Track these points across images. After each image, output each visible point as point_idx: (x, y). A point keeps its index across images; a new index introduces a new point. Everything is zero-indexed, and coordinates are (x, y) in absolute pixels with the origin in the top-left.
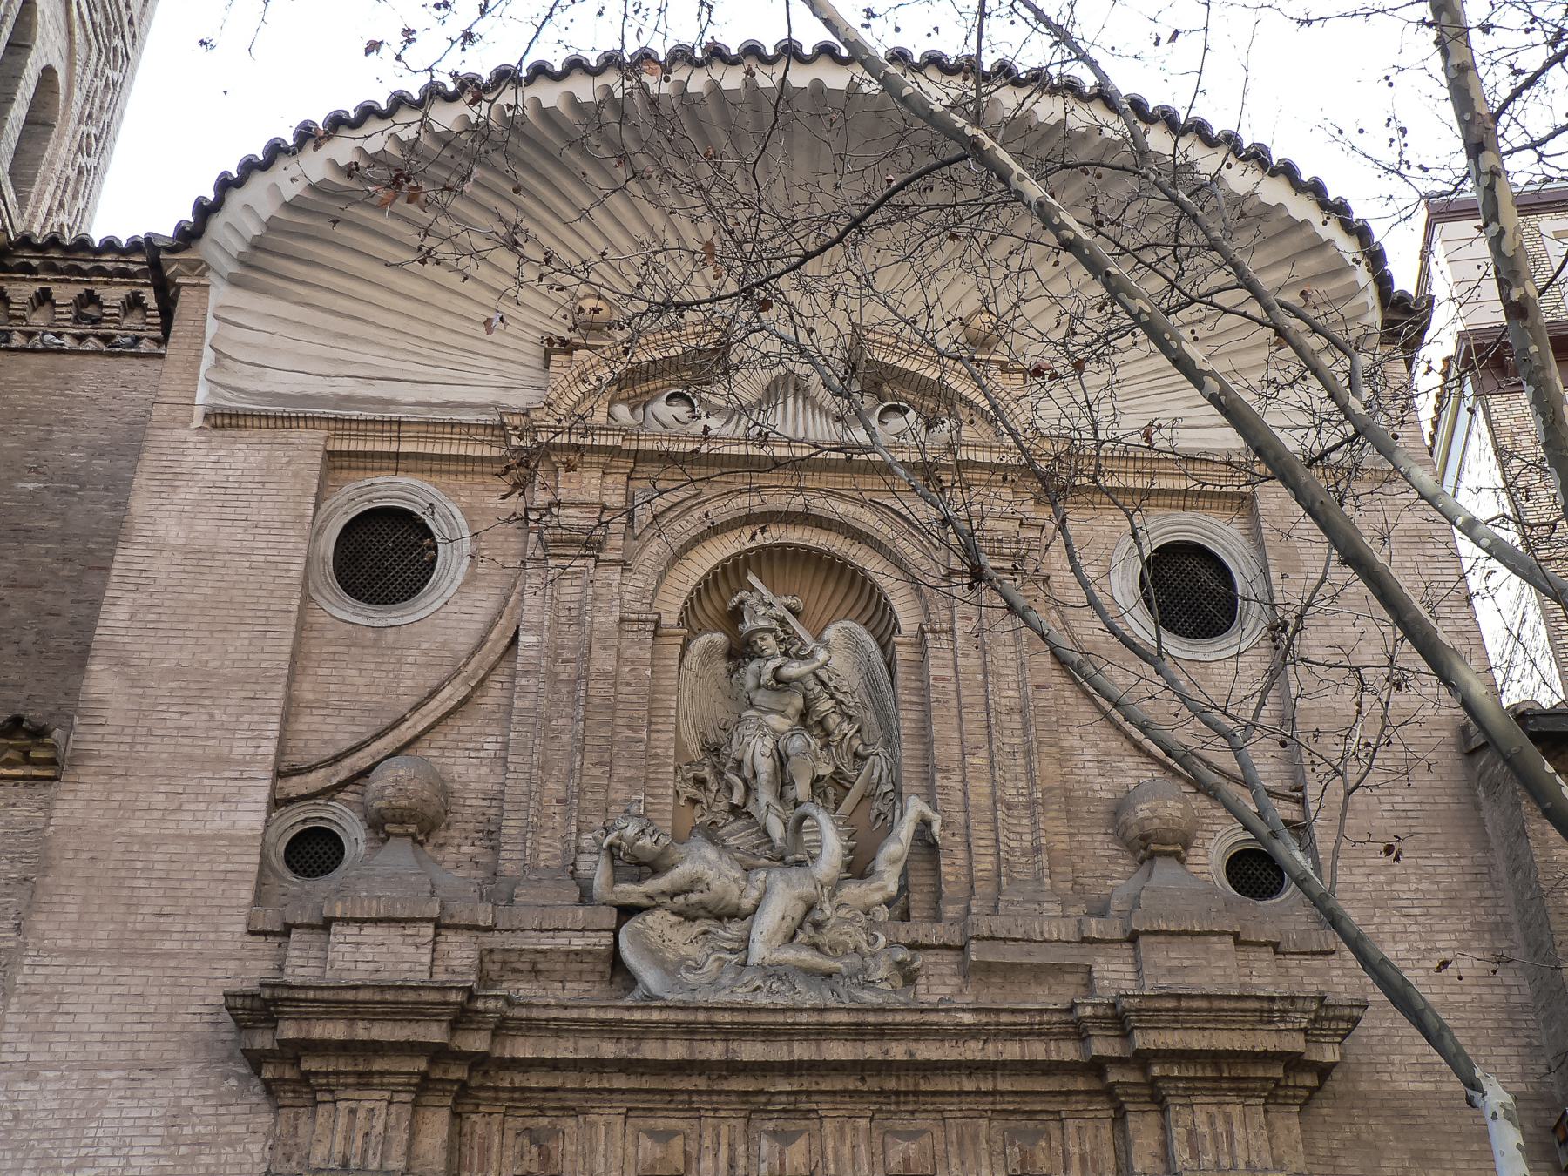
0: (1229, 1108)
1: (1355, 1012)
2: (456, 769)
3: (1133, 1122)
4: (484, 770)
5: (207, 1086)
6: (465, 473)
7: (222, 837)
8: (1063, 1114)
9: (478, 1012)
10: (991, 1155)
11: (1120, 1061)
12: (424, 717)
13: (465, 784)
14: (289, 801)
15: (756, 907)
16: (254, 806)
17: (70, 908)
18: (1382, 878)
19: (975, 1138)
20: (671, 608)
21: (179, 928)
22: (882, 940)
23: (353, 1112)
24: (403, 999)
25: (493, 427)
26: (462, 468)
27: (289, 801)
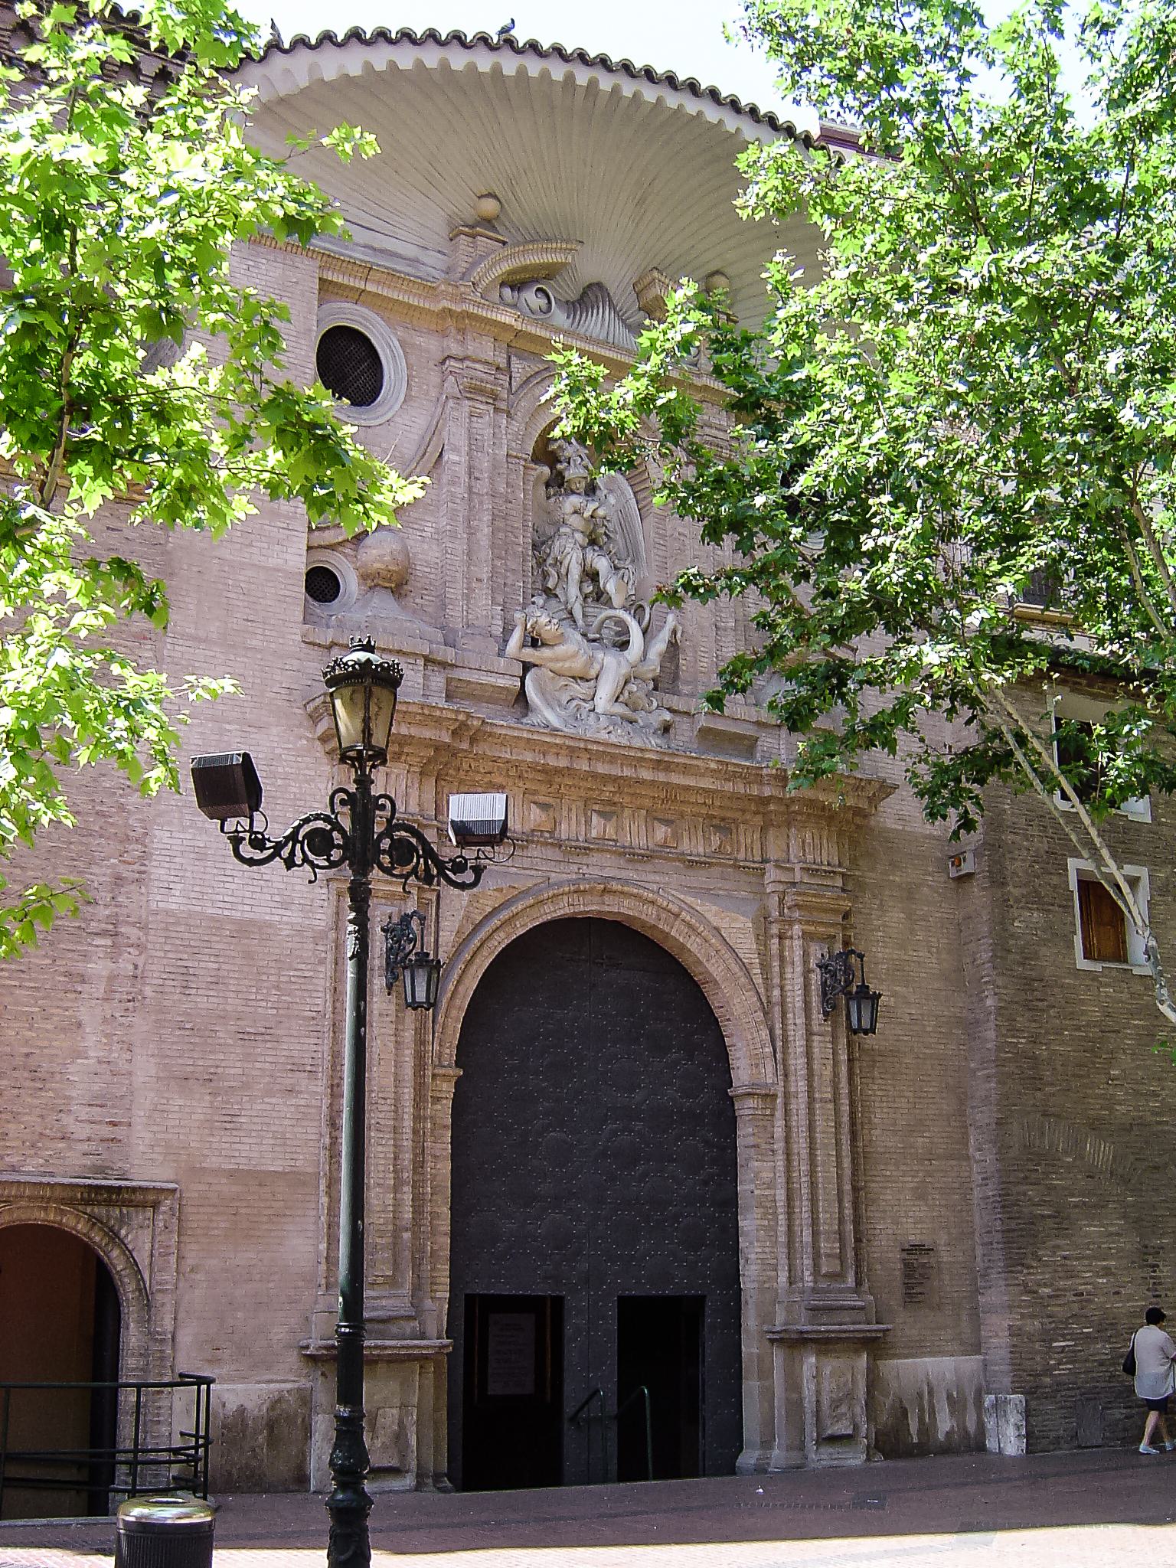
5: (289, 742)
7: (279, 570)
17: (191, 607)
21: (260, 631)
22: (655, 704)
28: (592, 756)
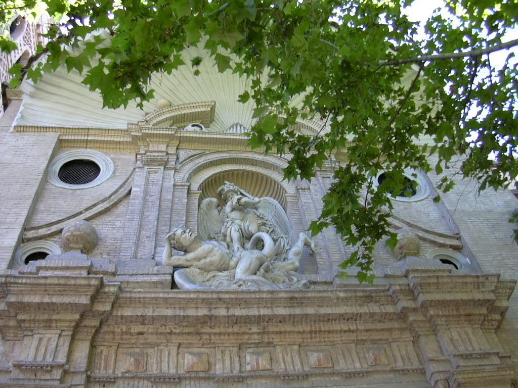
0: (467, 329)
1: (512, 284)
2: (102, 231)
3: (423, 340)
4: (114, 231)
6: (113, 148)
8: (390, 340)
9: (105, 293)
10: (359, 359)
11: (415, 310)
12: (90, 213)
13: (106, 236)
14: (29, 240)
15: (237, 265)
16: (13, 237)
18: (499, 258)
19: (350, 352)
20: (195, 186)
23: (41, 339)
24: (69, 283)
25: (125, 131)
26: (112, 147)
27: (29, 240)
28: (229, 304)
